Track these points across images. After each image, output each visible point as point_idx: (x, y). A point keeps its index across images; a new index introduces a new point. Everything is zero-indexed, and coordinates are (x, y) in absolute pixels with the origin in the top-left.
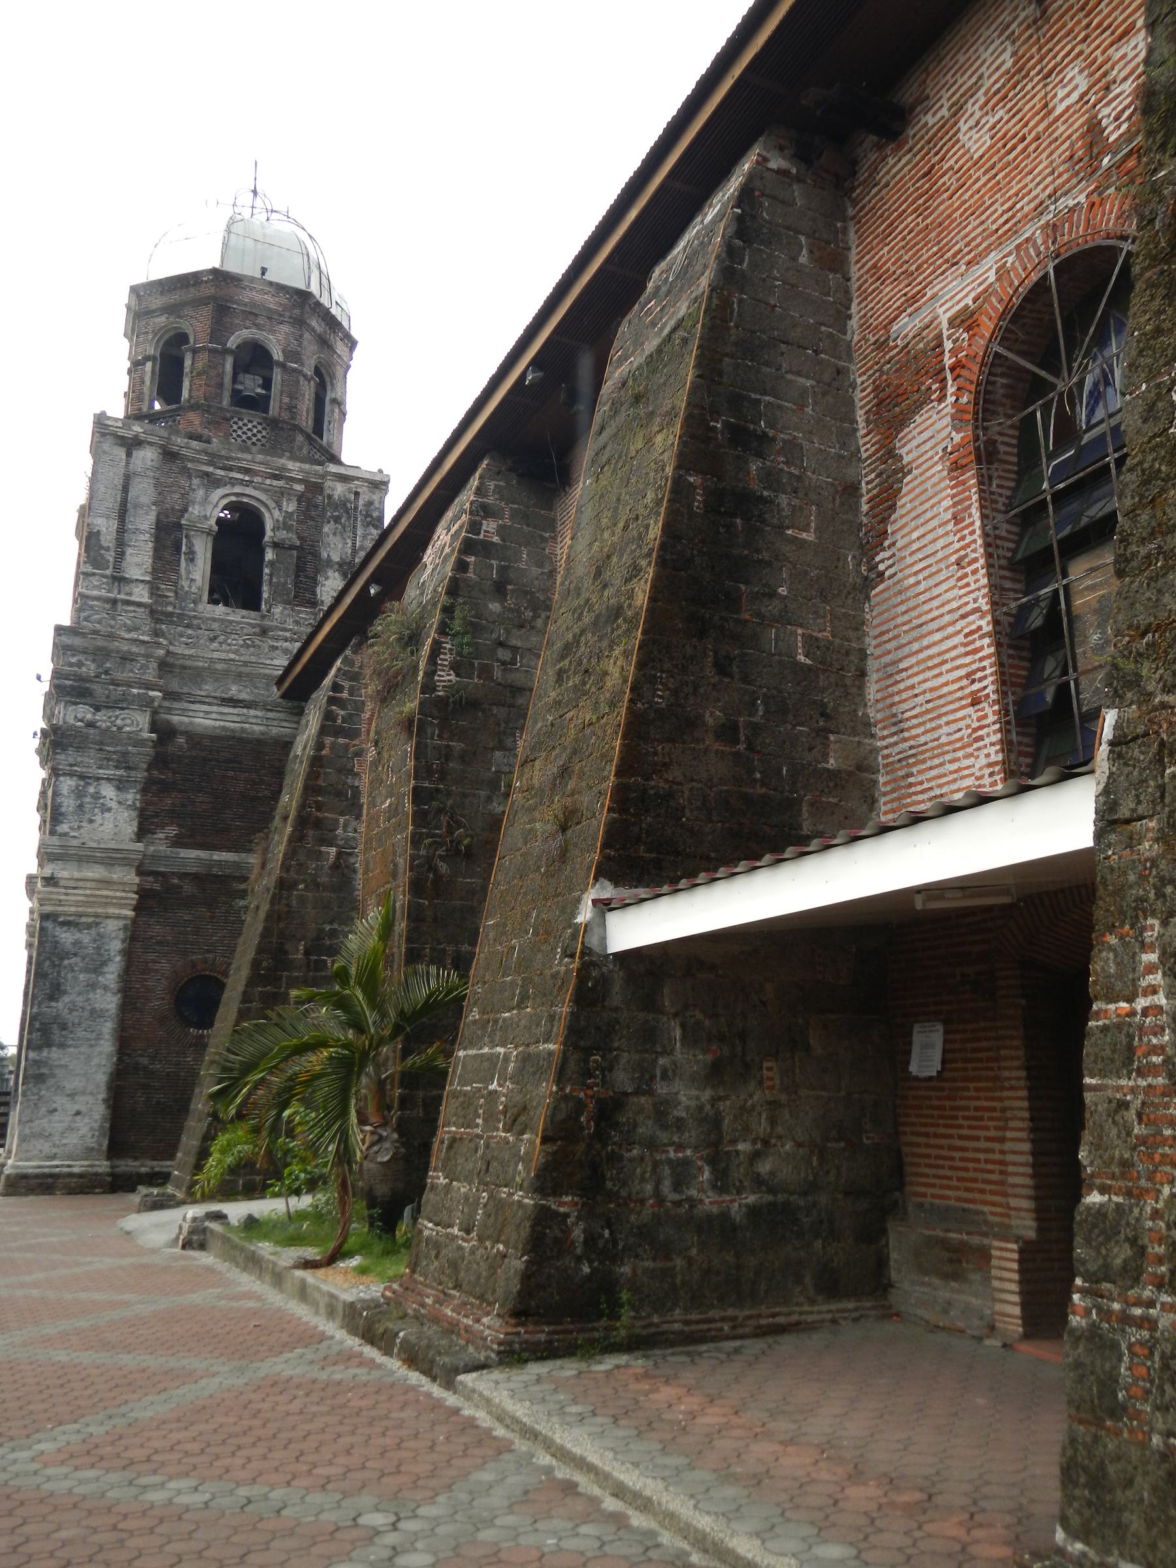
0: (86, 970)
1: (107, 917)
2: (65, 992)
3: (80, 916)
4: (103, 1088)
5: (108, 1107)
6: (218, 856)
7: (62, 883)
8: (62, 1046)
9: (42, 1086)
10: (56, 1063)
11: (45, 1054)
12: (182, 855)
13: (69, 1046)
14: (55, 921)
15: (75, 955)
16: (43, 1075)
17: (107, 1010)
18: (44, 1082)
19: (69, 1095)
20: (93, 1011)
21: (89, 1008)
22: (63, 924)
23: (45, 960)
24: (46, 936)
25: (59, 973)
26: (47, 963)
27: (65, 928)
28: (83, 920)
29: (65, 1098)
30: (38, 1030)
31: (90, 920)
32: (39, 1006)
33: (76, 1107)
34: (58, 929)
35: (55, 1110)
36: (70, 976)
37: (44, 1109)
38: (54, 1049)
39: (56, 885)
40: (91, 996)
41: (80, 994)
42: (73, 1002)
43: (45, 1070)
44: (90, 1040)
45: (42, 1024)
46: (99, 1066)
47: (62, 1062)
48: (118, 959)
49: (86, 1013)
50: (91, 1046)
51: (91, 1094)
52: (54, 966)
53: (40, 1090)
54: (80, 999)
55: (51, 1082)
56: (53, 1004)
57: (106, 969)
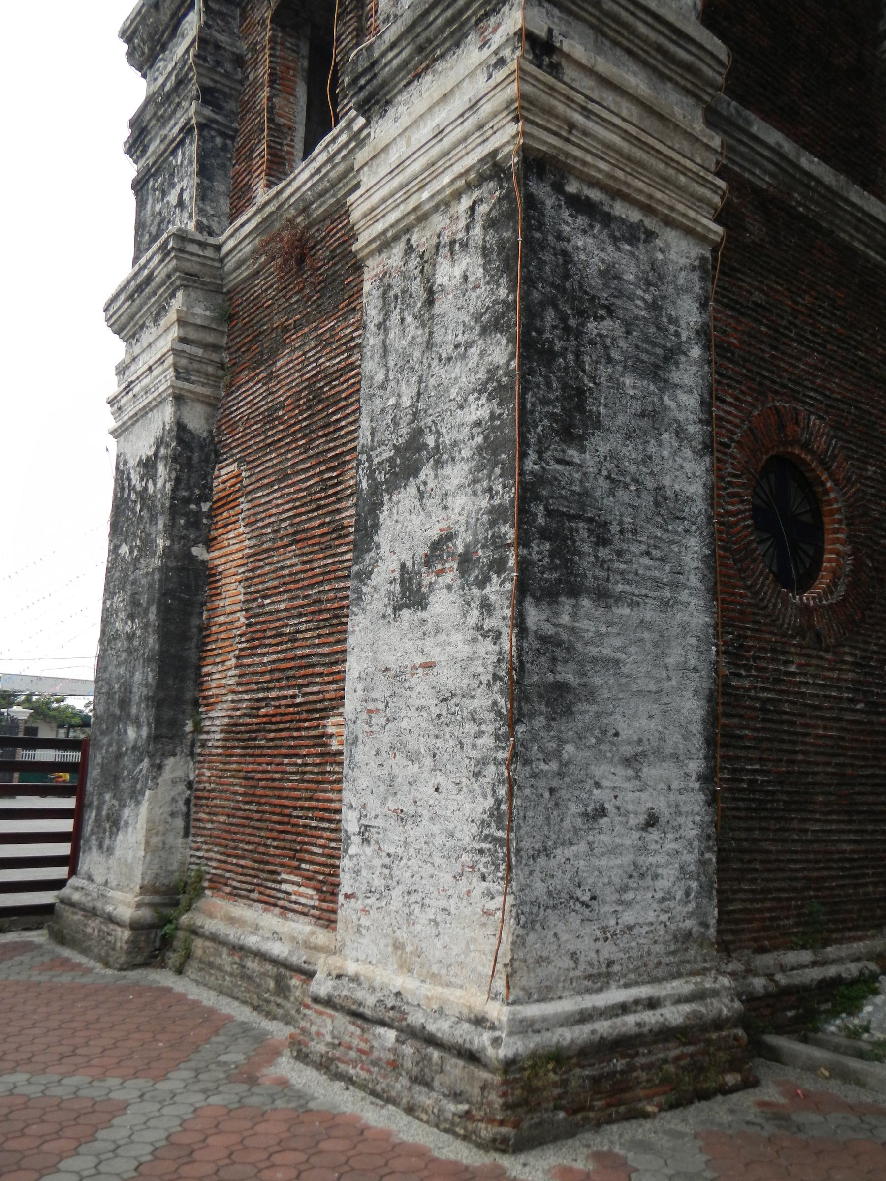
0: (636, 367)
1: (669, 222)
2: (598, 425)
3: (616, 194)
4: (697, 742)
5: (712, 800)
6: (809, 162)
7: (570, 73)
8: (603, 596)
9: (568, 729)
10: (593, 650)
11: (565, 619)
12: (754, 129)
13: (619, 599)
14: (558, 188)
15: (610, 311)
16: (562, 688)
17: (689, 500)
18: (568, 712)
19: (627, 762)
20: (660, 496)
21: (650, 484)
22: (580, 205)
23: (543, 304)
24: (541, 226)
25: (578, 355)
26: (550, 316)
27: (582, 221)
28: (619, 209)
29: (621, 771)
30: (545, 534)
31: (635, 216)
32: (540, 453)
33: (649, 800)
34: (565, 214)
35: (602, 811)
36: (604, 371)
37: (575, 808)
38: (586, 602)
39: (555, 69)
40: (652, 449)
41: (628, 437)
42: (613, 455)
43: (567, 675)
44: (658, 584)
45: (549, 513)
46: (683, 668)
47: (607, 651)
48: (696, 352)
49: (647, 500)
50: (665, 605)
51: (675, 757)
52: (567, 329)
53: (562, 742)
54: (629, 451)
55: (586, 712)
56: (573, 453)
57: (676, 376)
